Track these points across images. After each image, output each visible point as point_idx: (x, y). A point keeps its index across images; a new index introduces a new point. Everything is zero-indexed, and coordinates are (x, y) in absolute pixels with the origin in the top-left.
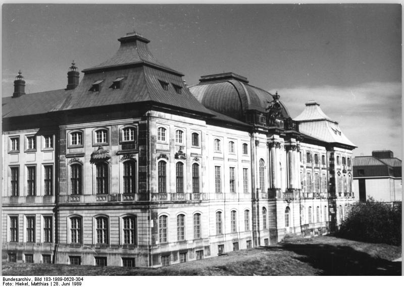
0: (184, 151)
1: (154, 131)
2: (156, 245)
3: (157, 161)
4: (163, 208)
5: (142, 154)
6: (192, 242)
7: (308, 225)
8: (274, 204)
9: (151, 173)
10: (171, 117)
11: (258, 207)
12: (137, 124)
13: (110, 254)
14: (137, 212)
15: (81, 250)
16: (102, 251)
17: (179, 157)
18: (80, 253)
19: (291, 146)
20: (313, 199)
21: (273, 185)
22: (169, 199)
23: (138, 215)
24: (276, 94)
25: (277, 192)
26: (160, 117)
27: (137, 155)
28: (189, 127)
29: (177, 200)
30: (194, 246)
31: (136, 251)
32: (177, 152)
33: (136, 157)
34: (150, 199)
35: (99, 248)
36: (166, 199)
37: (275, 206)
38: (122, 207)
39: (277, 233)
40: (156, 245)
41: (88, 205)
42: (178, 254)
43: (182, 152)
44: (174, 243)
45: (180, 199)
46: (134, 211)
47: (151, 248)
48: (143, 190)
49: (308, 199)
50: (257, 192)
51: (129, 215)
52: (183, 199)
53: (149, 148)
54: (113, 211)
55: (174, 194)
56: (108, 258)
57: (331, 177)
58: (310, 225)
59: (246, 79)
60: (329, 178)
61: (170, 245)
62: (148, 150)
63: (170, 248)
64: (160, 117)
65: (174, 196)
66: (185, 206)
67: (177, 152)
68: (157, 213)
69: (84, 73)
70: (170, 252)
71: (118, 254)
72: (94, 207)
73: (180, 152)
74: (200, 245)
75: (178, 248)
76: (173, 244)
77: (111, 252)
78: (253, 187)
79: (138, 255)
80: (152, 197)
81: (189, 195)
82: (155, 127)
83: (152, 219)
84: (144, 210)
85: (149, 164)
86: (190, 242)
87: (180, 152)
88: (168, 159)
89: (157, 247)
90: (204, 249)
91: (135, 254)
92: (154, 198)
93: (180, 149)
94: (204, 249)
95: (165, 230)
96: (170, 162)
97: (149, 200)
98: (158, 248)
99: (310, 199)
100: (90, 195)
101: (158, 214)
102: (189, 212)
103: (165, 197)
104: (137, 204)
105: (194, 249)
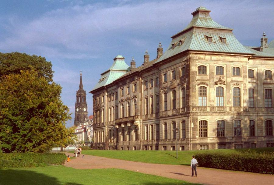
0: (223, 80)
1: (194, 68)
3: (197, 87)
4: (202, 116)
6: (231, 138)
9: (192, 94)
15: (166, 142)
17: (218, 83)
22: (208, 110)
26: (200, 59)
27: (185, 84)
28: (211, 63)
29: (217, 111)
33: (185, 86)
36: (206, 110)
38: (180, 116)
40: (196, 138)
42: (210, 144)
44: (213, 138)
47: (191, 139)
52: (223, 110)
54: (177, 119)
61: (208, 139)
64: (200, 59)
68: (197, 119)
69: (172, 38)
70: (209, 143)
72: (171, 118)
80: (193, 109)
82: (196, 65)
83: (192, 122)
88: (207, 85)
89: (197, 139)
90: (243, 143)
92: (195, 109)
93: (220, 78)
94: (243, 143)
95: (206, 130)
96: (210, 87)
98: (197, 140)
101: (198, 119)
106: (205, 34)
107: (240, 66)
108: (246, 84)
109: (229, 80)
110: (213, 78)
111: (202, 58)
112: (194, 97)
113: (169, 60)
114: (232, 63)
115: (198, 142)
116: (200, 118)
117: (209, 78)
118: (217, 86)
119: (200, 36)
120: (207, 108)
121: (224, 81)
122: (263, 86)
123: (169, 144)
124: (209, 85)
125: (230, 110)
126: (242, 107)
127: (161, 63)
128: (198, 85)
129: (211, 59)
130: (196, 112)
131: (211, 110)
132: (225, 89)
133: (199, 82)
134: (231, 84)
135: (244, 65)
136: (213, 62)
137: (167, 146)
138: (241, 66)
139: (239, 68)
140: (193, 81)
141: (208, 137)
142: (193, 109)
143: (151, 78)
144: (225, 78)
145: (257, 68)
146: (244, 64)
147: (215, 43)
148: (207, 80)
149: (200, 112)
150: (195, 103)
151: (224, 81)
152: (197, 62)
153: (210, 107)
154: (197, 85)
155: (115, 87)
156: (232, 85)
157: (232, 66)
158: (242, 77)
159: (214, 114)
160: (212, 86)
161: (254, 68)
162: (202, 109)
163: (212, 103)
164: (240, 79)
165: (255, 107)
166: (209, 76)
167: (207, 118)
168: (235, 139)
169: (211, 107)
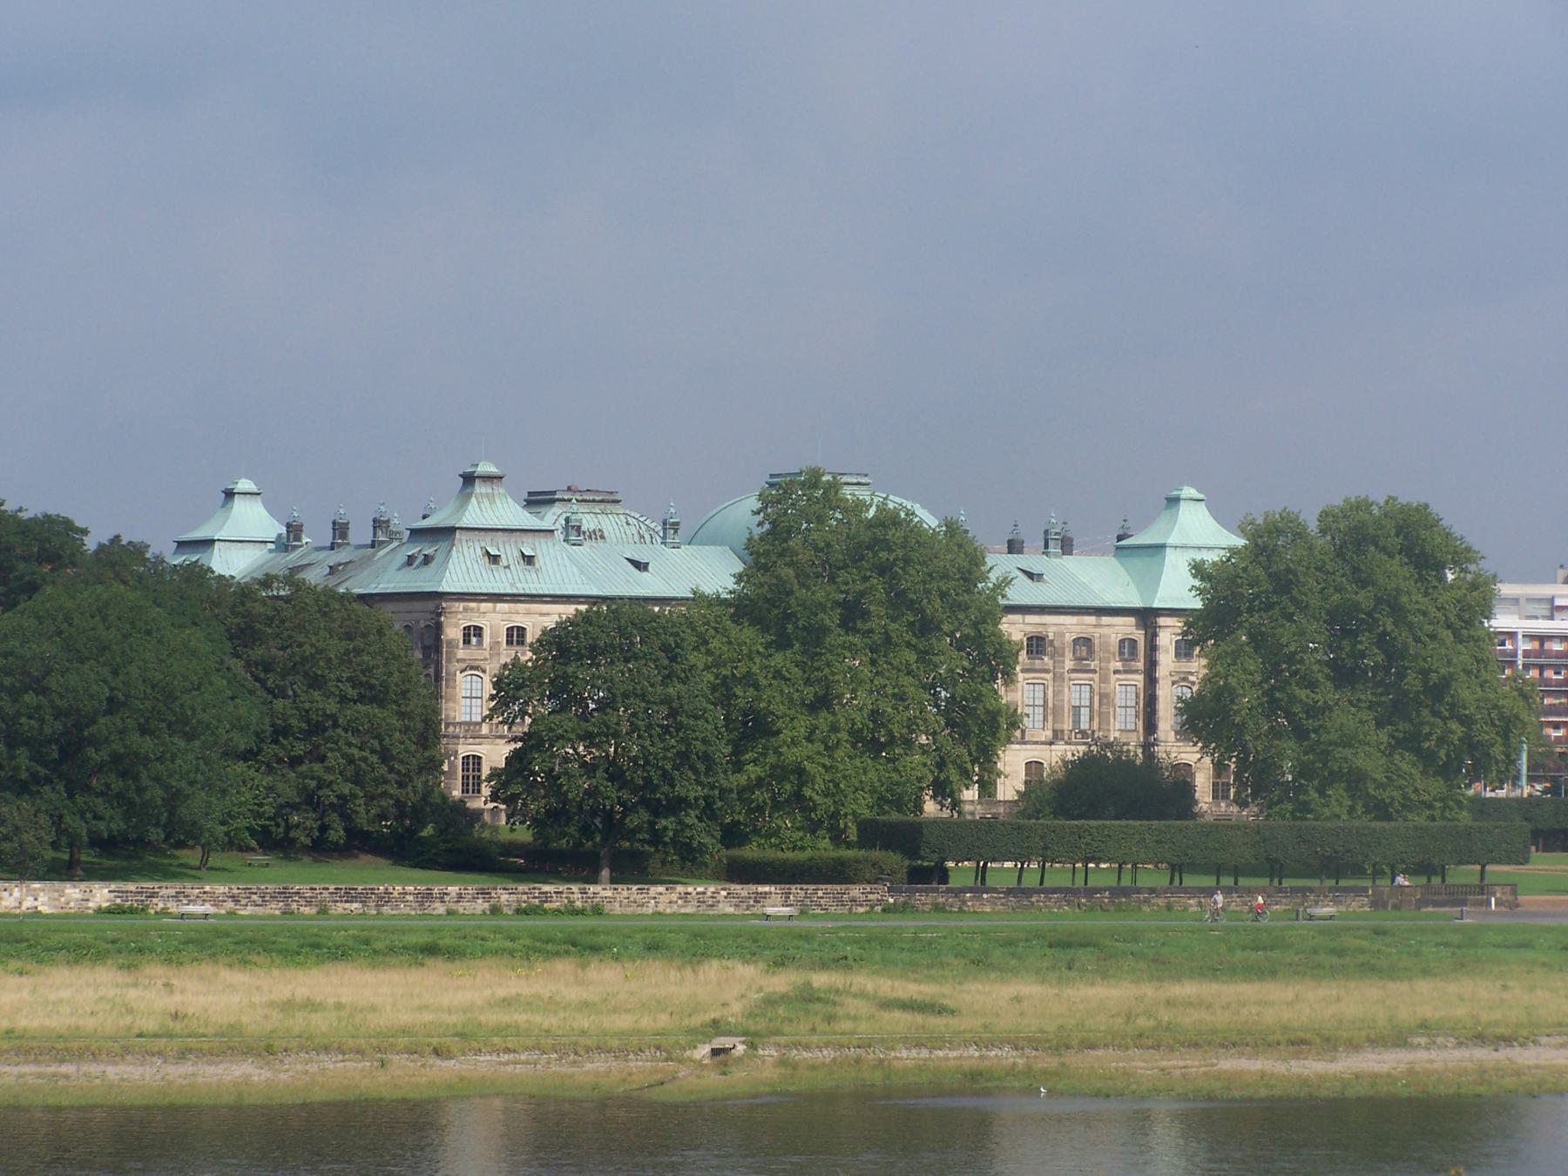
20: (1051, 743)
26: (465, 610)
36: (480, 730)
82: (457, 626)
88: (484, 671)
92: (451, 729)
106: (483, 544)
116: (464, 750)
117: (488, 656)
119: (472, 550)
124: (488, 671)
129: (494, 611)
130: (454, 737)
131: (491, 731)
133: (463, 665)
140: (449, 661)
142: (446, 728)
148: (486, 659)
149: (465, 737)
150: (452, 714)
152: (460, 616)
154: (458, 672)
167: (481, 750)
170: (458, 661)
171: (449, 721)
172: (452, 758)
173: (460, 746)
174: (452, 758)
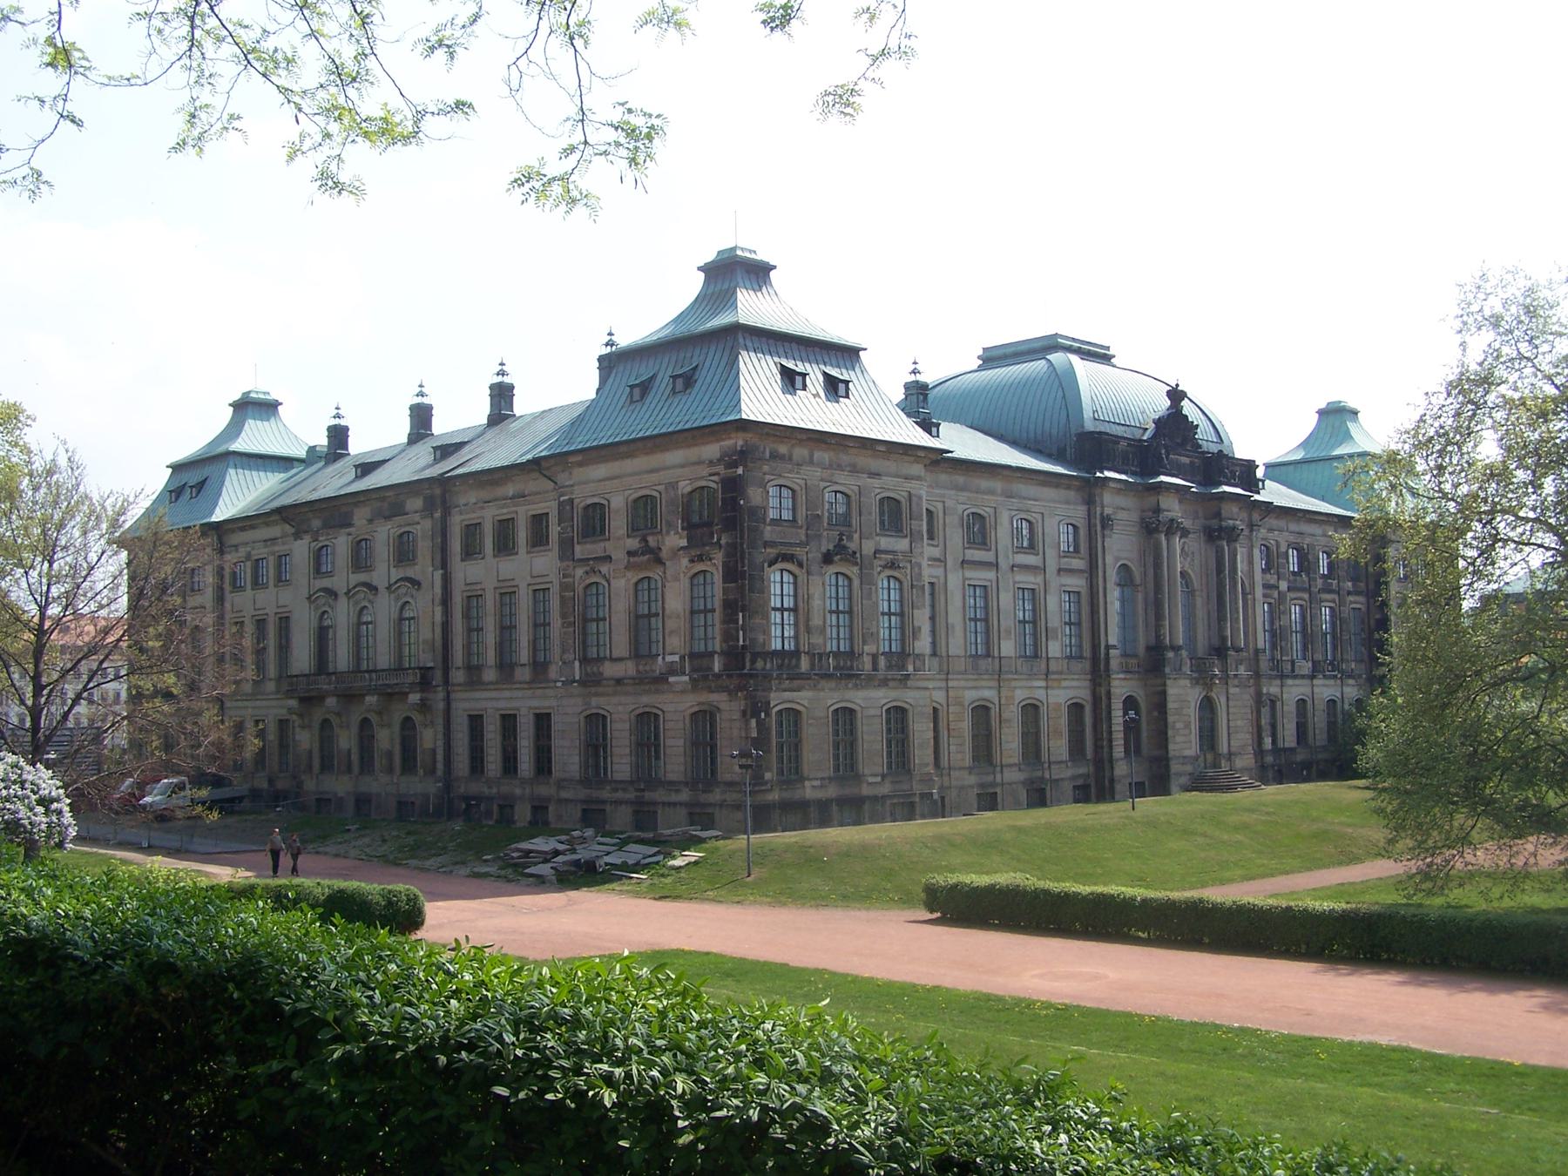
0: (853, 546)
2: (766, 783)
4: (785, 690)
5: (727, 555)
6: (879, 779)
7: (1292, 750)
8: (1160, 688)
10: (811, 456)
11: (1109, 694)
12: (715, 478)
13: (664, 804)
14: (719, 699)
16: (648, 795)
18: (604, 802)
19: (1221, 529)
21: (1158, 636)
22: (805, 664)
23: (722, 706)
24: (1177, 385)
25: (1170, 655)
26: (775, 456)
30: (886, 789)
31: (716, 796)
32: (831, 547)
34: (748, 665)
35: (643, 790)
36: (798, 666)
37: (1164, 693)
39: (1167, 767)
40: (766, 783)
41: (619, 681)
43: (845, 547)
44: (822, 779)
45: (842, 668)
46: (715, 698)
48: (731, 643)
49: (1296, 677)
50: (1107, 654)
51: (703, 708)
53: (742, 538)
55: (820, 655)
56: (659, 812)
57: (1378, 616)
58: (1298, 750)
59: (1108, 348)
60: (1372, 622)
62: (742, 544)
63: (809, 791)
64: (775, 456)
65: (820, 660)
66: (856, 687)
67: (831, 547)
71: (681, 804)
73: (840, 548)
74: (905, 787)
75: (832, 792)
76: (817, 783)
77: (666, 799)
78: (1097, 641)
79: (721, 806)
80: (753, 662)
81: (867, 660)
83: (752, 717)
84: (732, 693)
85: (743, 578)
86: (871, 780)
87: (840, 548)
88: (800, 565)
89: (769, 786)
91: (715, 805)
92: (759, 664)
93: (840, 540)
97: (744, 668)
98: (771, 790)
99: (1303, 677)
100: (620, 659)
102: (871, 701)
103: (794, 661)
104: (718, 676)
105: (883, 797)
107: (901, 496)
108: (920, 566)
109: (868, 547)
110: (819, 537)
111: (784, 455)
112: (757, 612)
113: (623, 449)
114: (876, 482)
115: (774, 796)
117: (804, 538)
118: (832, 569)
120: (799, 659)
121: (855, 553)
122: (1010, 575)
123: (618, 803)
125: (875, 668)
126: (909, 655)
127: (579, 458)
128: (770, 566)
129: (811, 462)
130: (765, 677)
131: (812, 665)
132: (856, 583)
133: (772, 552)
134: (876, 562)
135: (913, 492)
136: (818, 473)
137: (608, 808)
138: (905, 494)
139: (898, 502)
141: (805, 775)
143: (505, 511)
144: (856, 536)
145: (940, 506)
146: (912, 486)
147: (817, 395)
148: (800, 545)
149: (779, 677)
151: (855, 553)
152: (766, 468)
153: (810, 654)
154: (766, 565)
155: (275, 531)
156: (879, 569)
157: (878, 491)
158: (906, 536)
159: (823, 683)
160: (815, 568)
161: (934, 503)
162: (783, 660)
163: (816, 640)
164: (902, 544)
165: (939, 653)
166: (805, 528)
168: (892, 782)
169: (814, 654)
170: (766, 544)
171: (758, 649)
172: (763, 715)
173: (772, 695)
174: (763, 715)
